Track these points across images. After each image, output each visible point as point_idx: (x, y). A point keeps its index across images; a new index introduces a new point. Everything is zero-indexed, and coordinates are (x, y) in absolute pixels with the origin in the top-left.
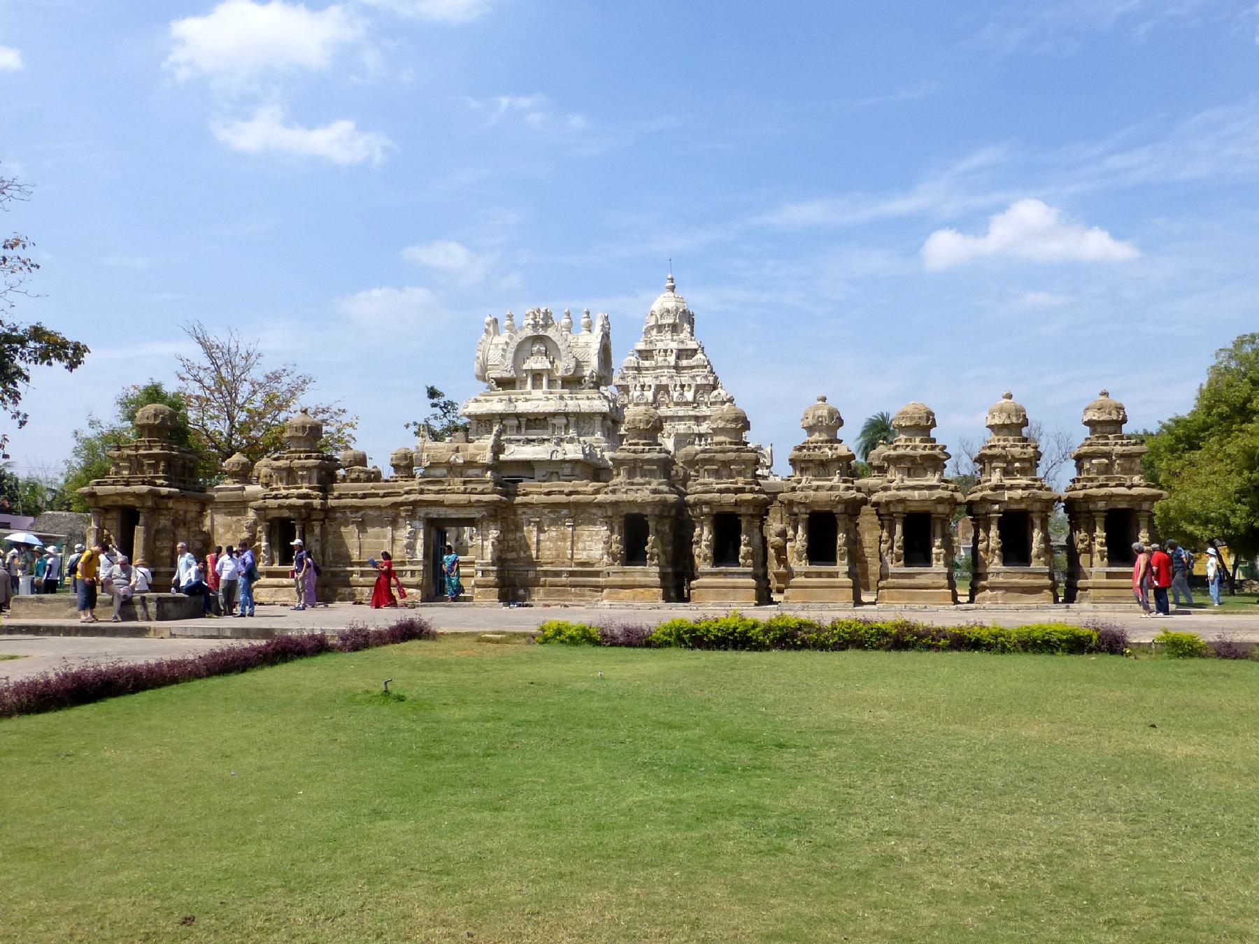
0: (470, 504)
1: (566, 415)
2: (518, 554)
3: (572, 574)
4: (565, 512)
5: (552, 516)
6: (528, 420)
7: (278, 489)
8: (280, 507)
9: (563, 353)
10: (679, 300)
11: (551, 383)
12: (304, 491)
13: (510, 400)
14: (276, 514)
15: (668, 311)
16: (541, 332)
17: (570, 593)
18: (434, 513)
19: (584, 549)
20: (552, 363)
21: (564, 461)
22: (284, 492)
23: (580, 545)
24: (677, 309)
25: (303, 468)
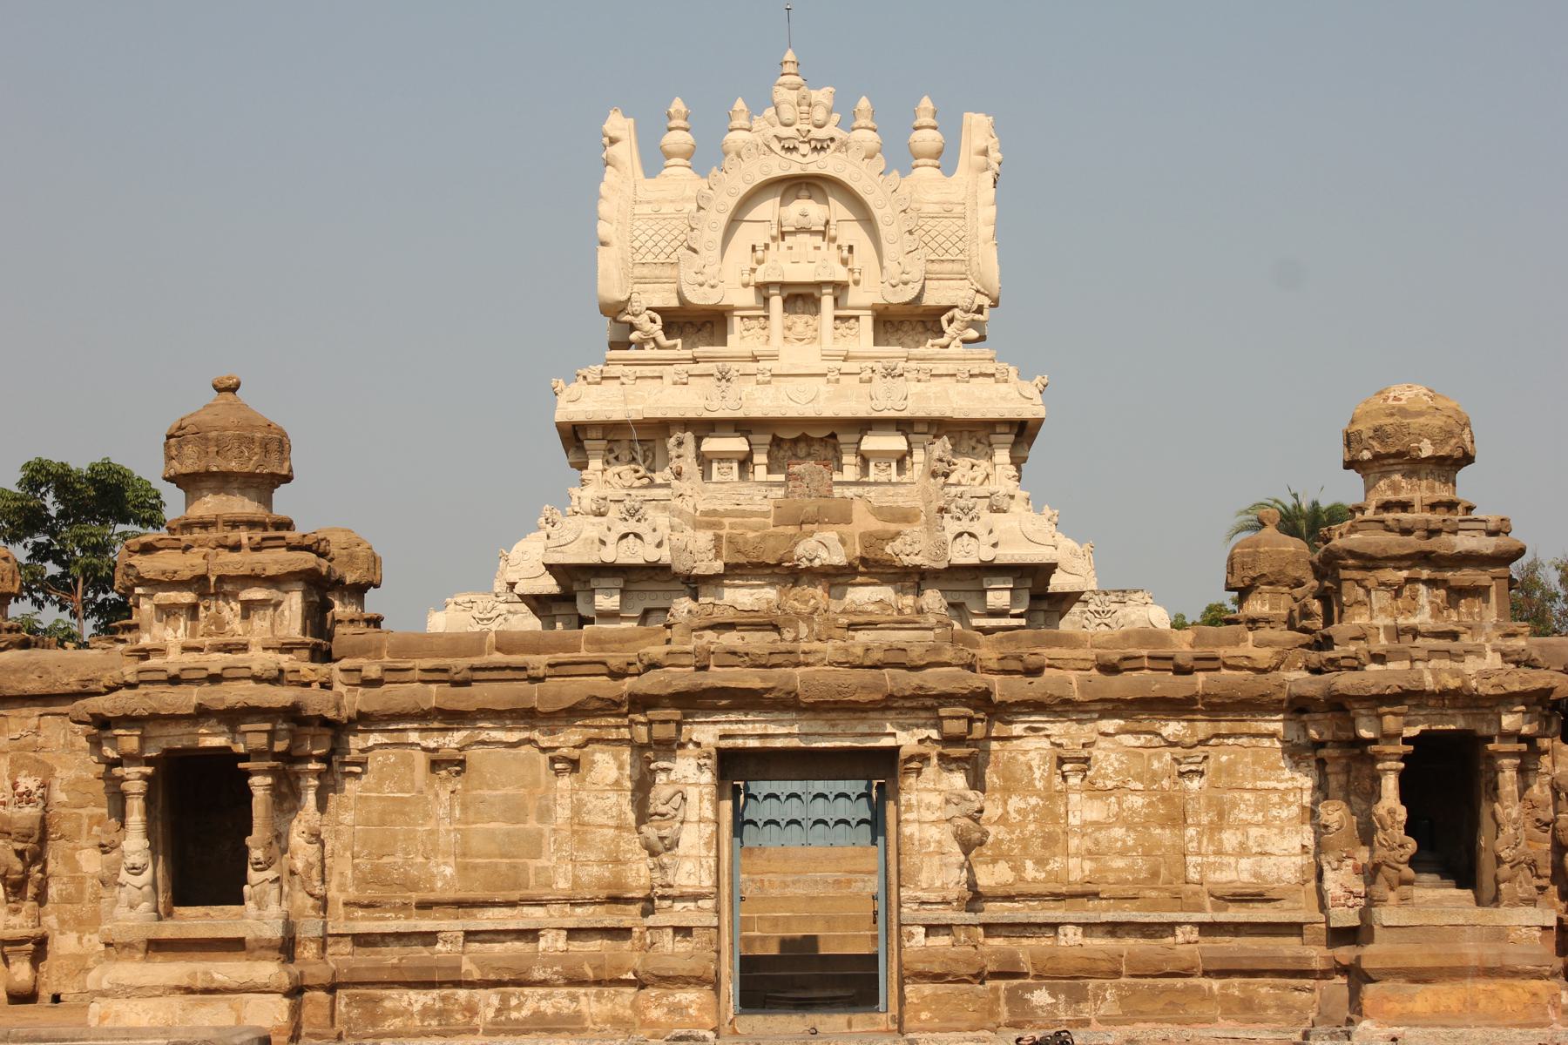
0: (888, 704)
1: (903, 425)
2: (1017, 869)
3: (1207, 929)
4: (1172, 728)
5: (1129, 740)
6: (777, 442)
7: (160, 651)
8: (202, 714)
12: (260, 660)
13: (724, 377)
14: (177, 738)
17: (1207, 996)
18: (752, 731)
19: (1243, 851)
22: (175, 660)
23: (1230, 839)
25: (253, 579)
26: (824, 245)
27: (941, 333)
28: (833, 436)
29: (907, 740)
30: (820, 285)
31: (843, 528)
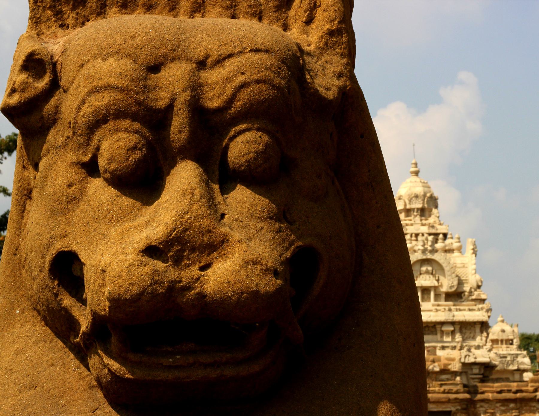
1: (453, 323)
5: (503, 408)
9: (447, 273)
10: (426, 185)
11: (437, 296)
15: (417, 196)
16: (429, 256)
20: (438, 280)
21: (474, 364)
24: (425, 195)
26: (431, 276)
27: (461, 298)
28: (435, 325)
29: (453, 409)
30: (431, 287)
31: (440, 363)
